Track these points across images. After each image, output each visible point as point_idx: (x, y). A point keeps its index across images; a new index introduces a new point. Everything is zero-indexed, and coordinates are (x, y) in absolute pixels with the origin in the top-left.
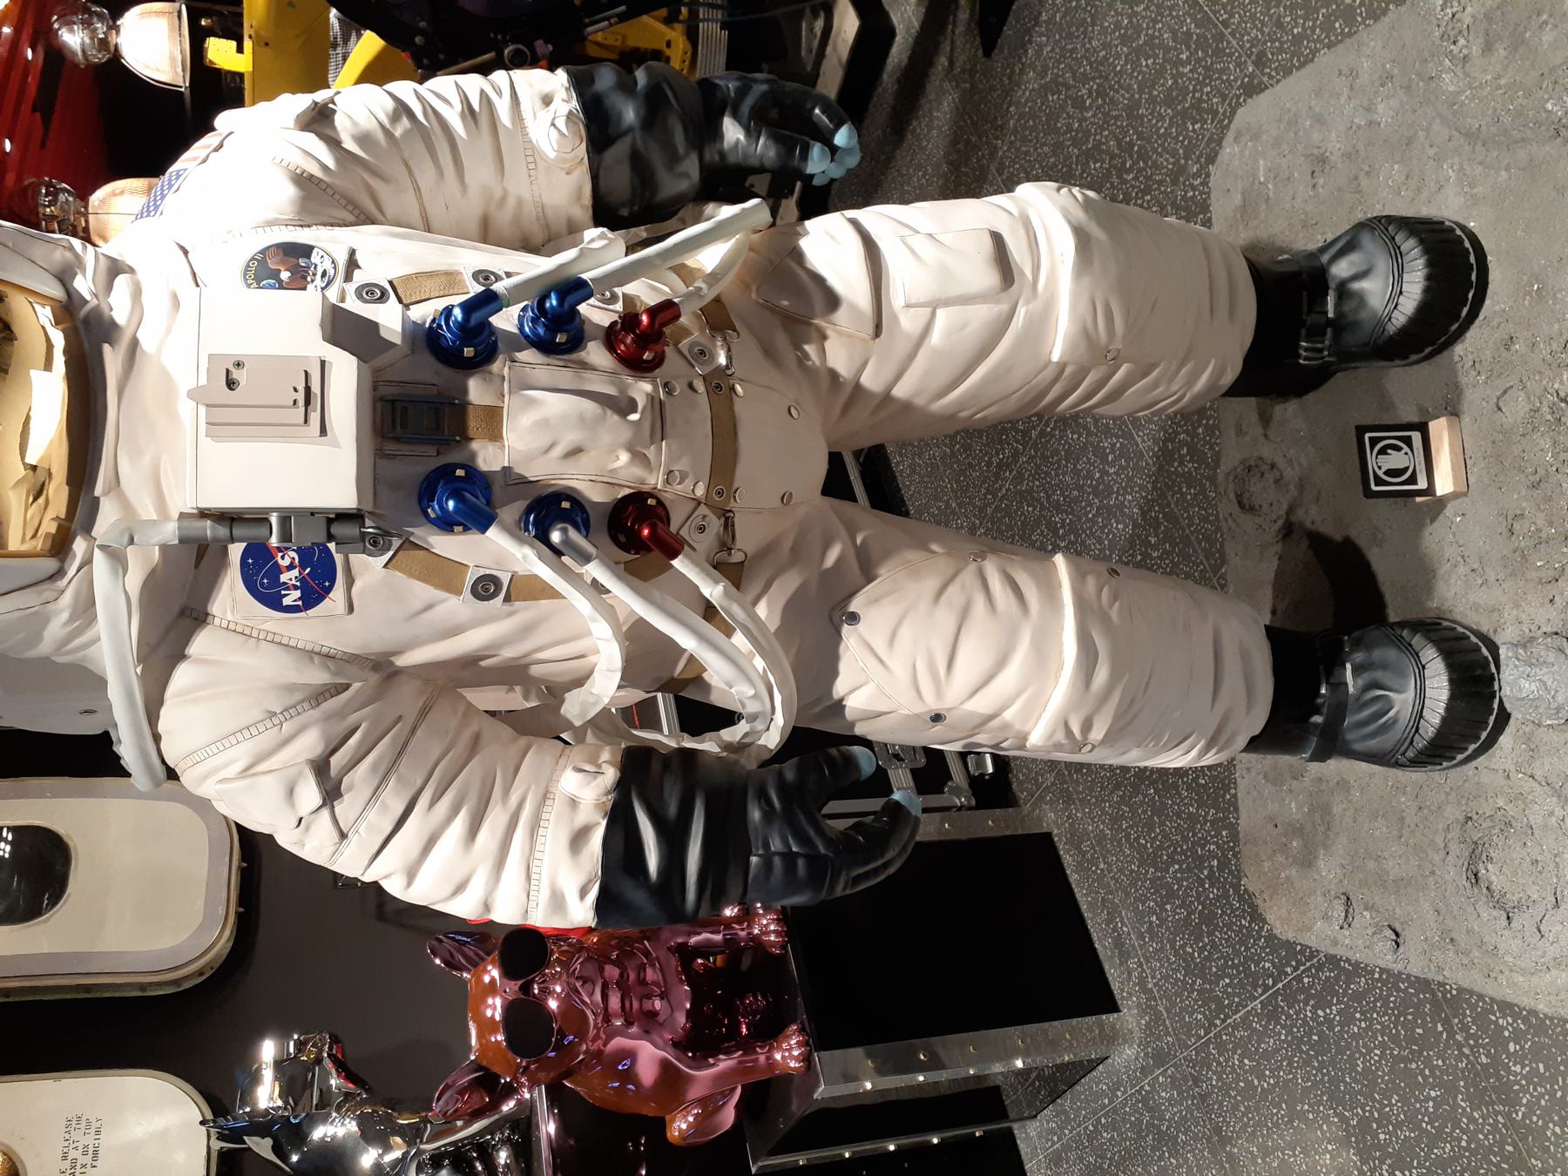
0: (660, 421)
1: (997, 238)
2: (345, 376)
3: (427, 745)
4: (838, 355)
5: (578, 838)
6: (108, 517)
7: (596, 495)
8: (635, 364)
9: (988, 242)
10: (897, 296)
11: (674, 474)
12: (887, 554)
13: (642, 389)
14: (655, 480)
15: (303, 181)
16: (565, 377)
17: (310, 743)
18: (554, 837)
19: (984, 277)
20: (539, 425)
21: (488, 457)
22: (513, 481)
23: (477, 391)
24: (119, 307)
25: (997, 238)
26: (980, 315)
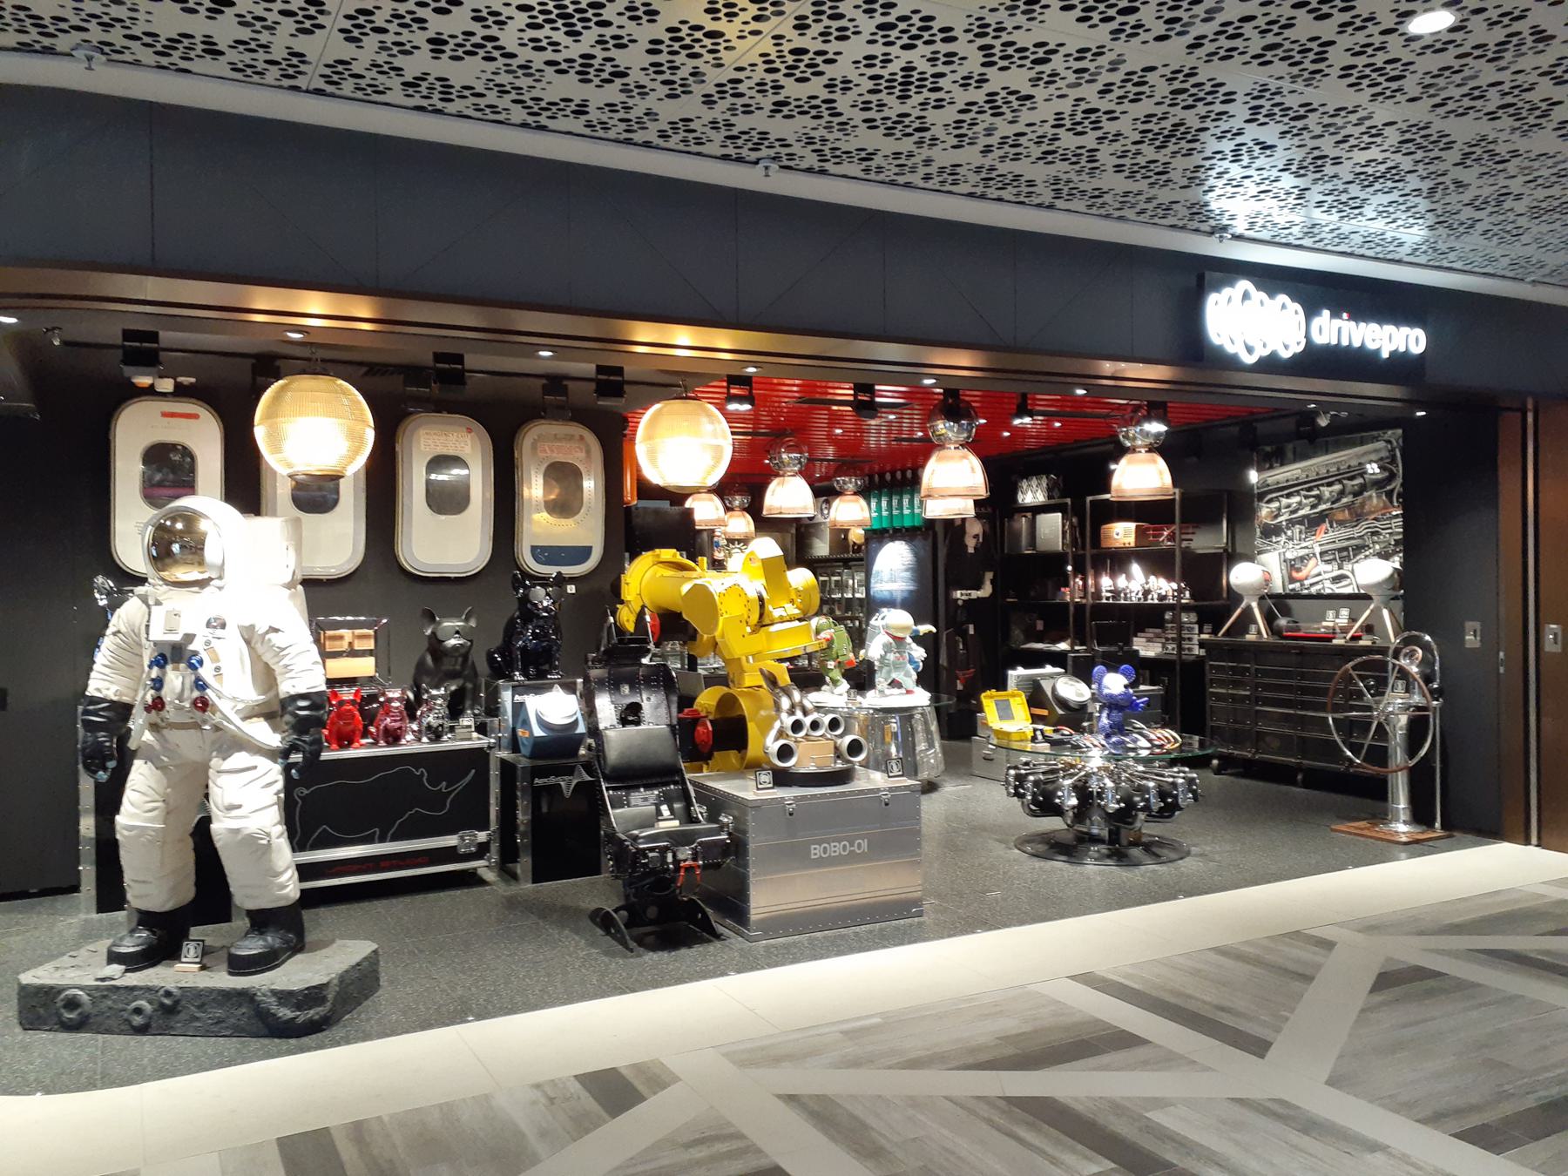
0: (180, 708)
1: (240, 807)
2: (177, 638)
3: (126, 655)
4: (215, 762)
5: (98, 690)
6: (165, 588)
7: (163, 693)
8: (194, 703)
9: (236, 803)
10: (224, 777)
11: (170, 713)
12: (165, 774)
13: (187, 705)
14: (167, 707)
15: (252, 627)
16: (188, 686)
17: (123, 629)
18: (101, 685)
19: (227, 802)
20: (175, 679)
21: (169, 667)
22: (164, 674)
23: (182, 665)
24: (207, 589)
25: (240, 807)
26: (219, 802)
